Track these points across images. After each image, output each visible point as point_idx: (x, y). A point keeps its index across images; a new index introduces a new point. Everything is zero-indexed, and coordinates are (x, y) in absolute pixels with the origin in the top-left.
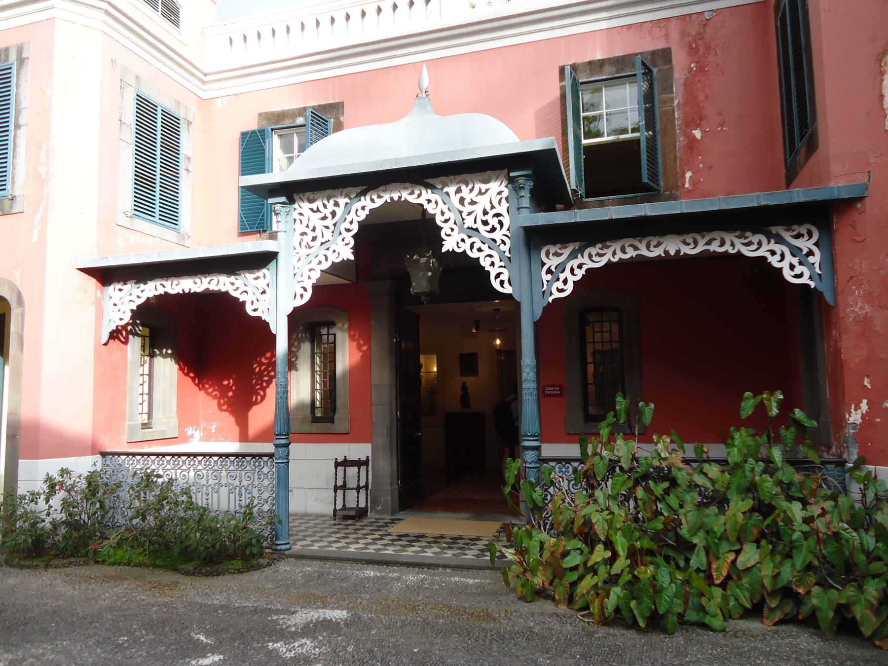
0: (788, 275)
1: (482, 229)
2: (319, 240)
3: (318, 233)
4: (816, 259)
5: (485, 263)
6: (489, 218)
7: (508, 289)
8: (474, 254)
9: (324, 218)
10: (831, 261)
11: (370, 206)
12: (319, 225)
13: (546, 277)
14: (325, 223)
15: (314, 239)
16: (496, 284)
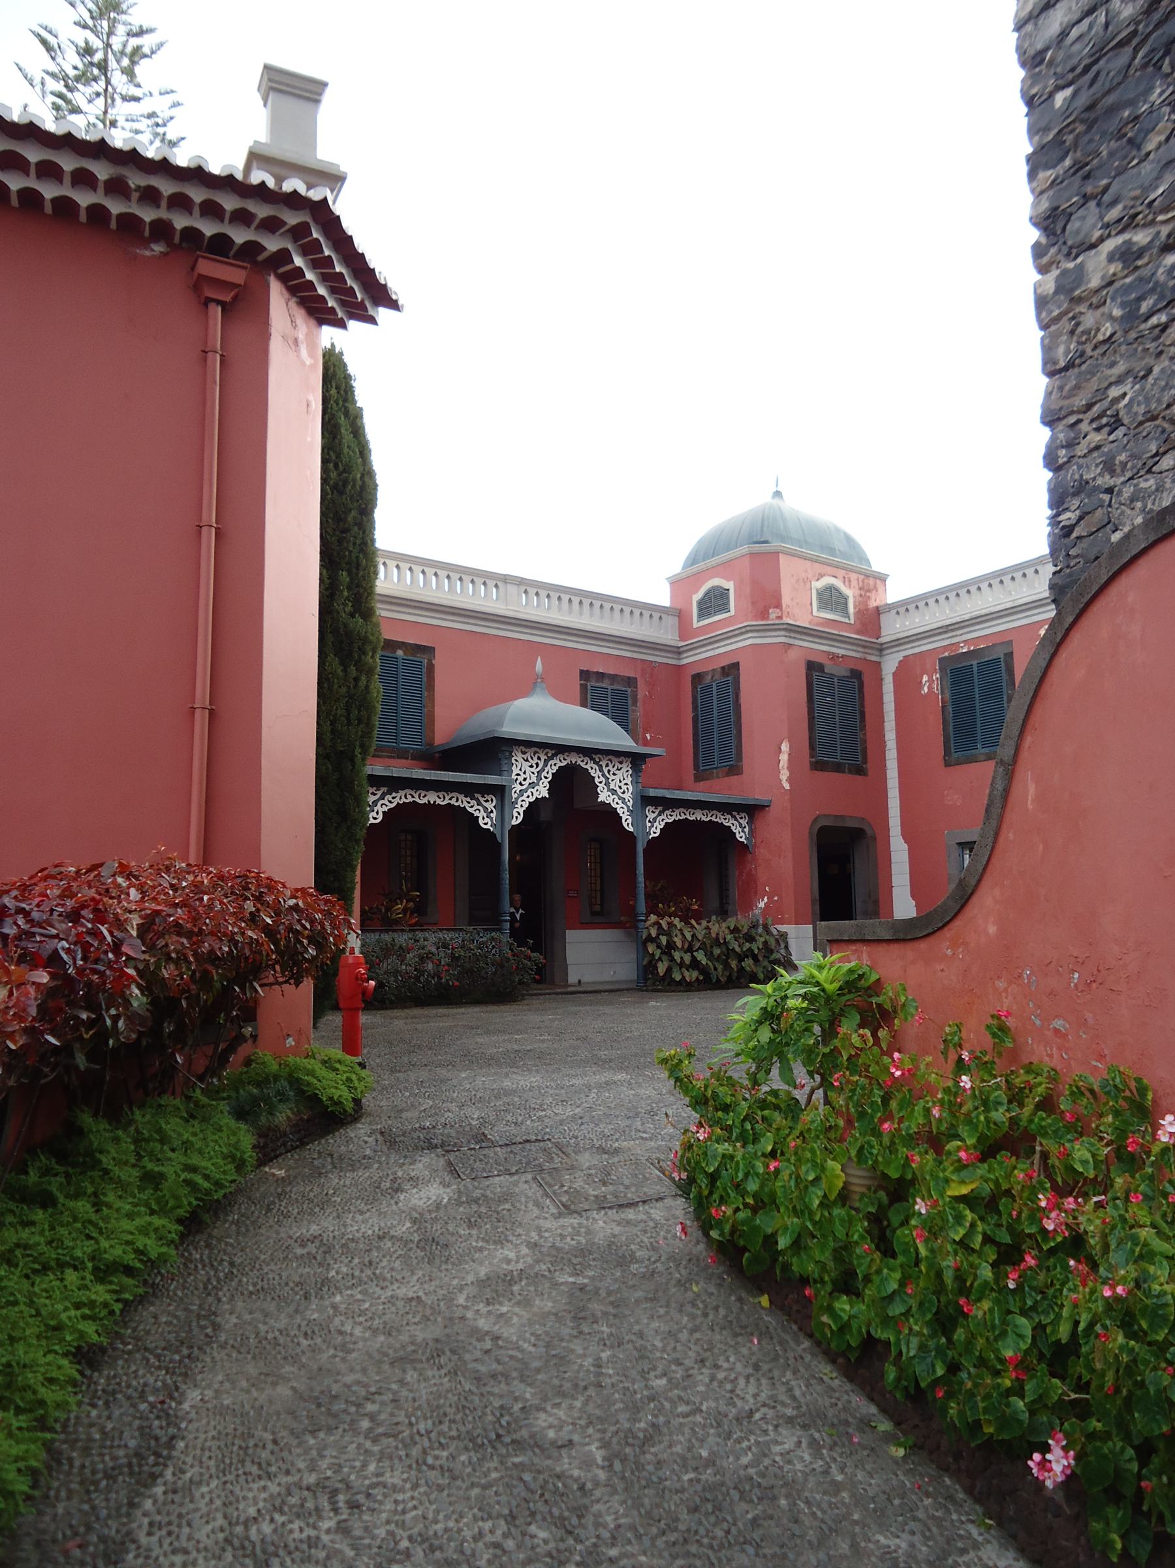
0: (738, 836)
1: (619, 791)
3: (527, 775)
4: (746, 830)
5: (620, 811)
6: (622, 784)
7: (631, 829)
8: (614, 806)
9: (531, 766)
11: (560, 764)
12: (529, 770)
13: (649, 825)
14: (533, 770)
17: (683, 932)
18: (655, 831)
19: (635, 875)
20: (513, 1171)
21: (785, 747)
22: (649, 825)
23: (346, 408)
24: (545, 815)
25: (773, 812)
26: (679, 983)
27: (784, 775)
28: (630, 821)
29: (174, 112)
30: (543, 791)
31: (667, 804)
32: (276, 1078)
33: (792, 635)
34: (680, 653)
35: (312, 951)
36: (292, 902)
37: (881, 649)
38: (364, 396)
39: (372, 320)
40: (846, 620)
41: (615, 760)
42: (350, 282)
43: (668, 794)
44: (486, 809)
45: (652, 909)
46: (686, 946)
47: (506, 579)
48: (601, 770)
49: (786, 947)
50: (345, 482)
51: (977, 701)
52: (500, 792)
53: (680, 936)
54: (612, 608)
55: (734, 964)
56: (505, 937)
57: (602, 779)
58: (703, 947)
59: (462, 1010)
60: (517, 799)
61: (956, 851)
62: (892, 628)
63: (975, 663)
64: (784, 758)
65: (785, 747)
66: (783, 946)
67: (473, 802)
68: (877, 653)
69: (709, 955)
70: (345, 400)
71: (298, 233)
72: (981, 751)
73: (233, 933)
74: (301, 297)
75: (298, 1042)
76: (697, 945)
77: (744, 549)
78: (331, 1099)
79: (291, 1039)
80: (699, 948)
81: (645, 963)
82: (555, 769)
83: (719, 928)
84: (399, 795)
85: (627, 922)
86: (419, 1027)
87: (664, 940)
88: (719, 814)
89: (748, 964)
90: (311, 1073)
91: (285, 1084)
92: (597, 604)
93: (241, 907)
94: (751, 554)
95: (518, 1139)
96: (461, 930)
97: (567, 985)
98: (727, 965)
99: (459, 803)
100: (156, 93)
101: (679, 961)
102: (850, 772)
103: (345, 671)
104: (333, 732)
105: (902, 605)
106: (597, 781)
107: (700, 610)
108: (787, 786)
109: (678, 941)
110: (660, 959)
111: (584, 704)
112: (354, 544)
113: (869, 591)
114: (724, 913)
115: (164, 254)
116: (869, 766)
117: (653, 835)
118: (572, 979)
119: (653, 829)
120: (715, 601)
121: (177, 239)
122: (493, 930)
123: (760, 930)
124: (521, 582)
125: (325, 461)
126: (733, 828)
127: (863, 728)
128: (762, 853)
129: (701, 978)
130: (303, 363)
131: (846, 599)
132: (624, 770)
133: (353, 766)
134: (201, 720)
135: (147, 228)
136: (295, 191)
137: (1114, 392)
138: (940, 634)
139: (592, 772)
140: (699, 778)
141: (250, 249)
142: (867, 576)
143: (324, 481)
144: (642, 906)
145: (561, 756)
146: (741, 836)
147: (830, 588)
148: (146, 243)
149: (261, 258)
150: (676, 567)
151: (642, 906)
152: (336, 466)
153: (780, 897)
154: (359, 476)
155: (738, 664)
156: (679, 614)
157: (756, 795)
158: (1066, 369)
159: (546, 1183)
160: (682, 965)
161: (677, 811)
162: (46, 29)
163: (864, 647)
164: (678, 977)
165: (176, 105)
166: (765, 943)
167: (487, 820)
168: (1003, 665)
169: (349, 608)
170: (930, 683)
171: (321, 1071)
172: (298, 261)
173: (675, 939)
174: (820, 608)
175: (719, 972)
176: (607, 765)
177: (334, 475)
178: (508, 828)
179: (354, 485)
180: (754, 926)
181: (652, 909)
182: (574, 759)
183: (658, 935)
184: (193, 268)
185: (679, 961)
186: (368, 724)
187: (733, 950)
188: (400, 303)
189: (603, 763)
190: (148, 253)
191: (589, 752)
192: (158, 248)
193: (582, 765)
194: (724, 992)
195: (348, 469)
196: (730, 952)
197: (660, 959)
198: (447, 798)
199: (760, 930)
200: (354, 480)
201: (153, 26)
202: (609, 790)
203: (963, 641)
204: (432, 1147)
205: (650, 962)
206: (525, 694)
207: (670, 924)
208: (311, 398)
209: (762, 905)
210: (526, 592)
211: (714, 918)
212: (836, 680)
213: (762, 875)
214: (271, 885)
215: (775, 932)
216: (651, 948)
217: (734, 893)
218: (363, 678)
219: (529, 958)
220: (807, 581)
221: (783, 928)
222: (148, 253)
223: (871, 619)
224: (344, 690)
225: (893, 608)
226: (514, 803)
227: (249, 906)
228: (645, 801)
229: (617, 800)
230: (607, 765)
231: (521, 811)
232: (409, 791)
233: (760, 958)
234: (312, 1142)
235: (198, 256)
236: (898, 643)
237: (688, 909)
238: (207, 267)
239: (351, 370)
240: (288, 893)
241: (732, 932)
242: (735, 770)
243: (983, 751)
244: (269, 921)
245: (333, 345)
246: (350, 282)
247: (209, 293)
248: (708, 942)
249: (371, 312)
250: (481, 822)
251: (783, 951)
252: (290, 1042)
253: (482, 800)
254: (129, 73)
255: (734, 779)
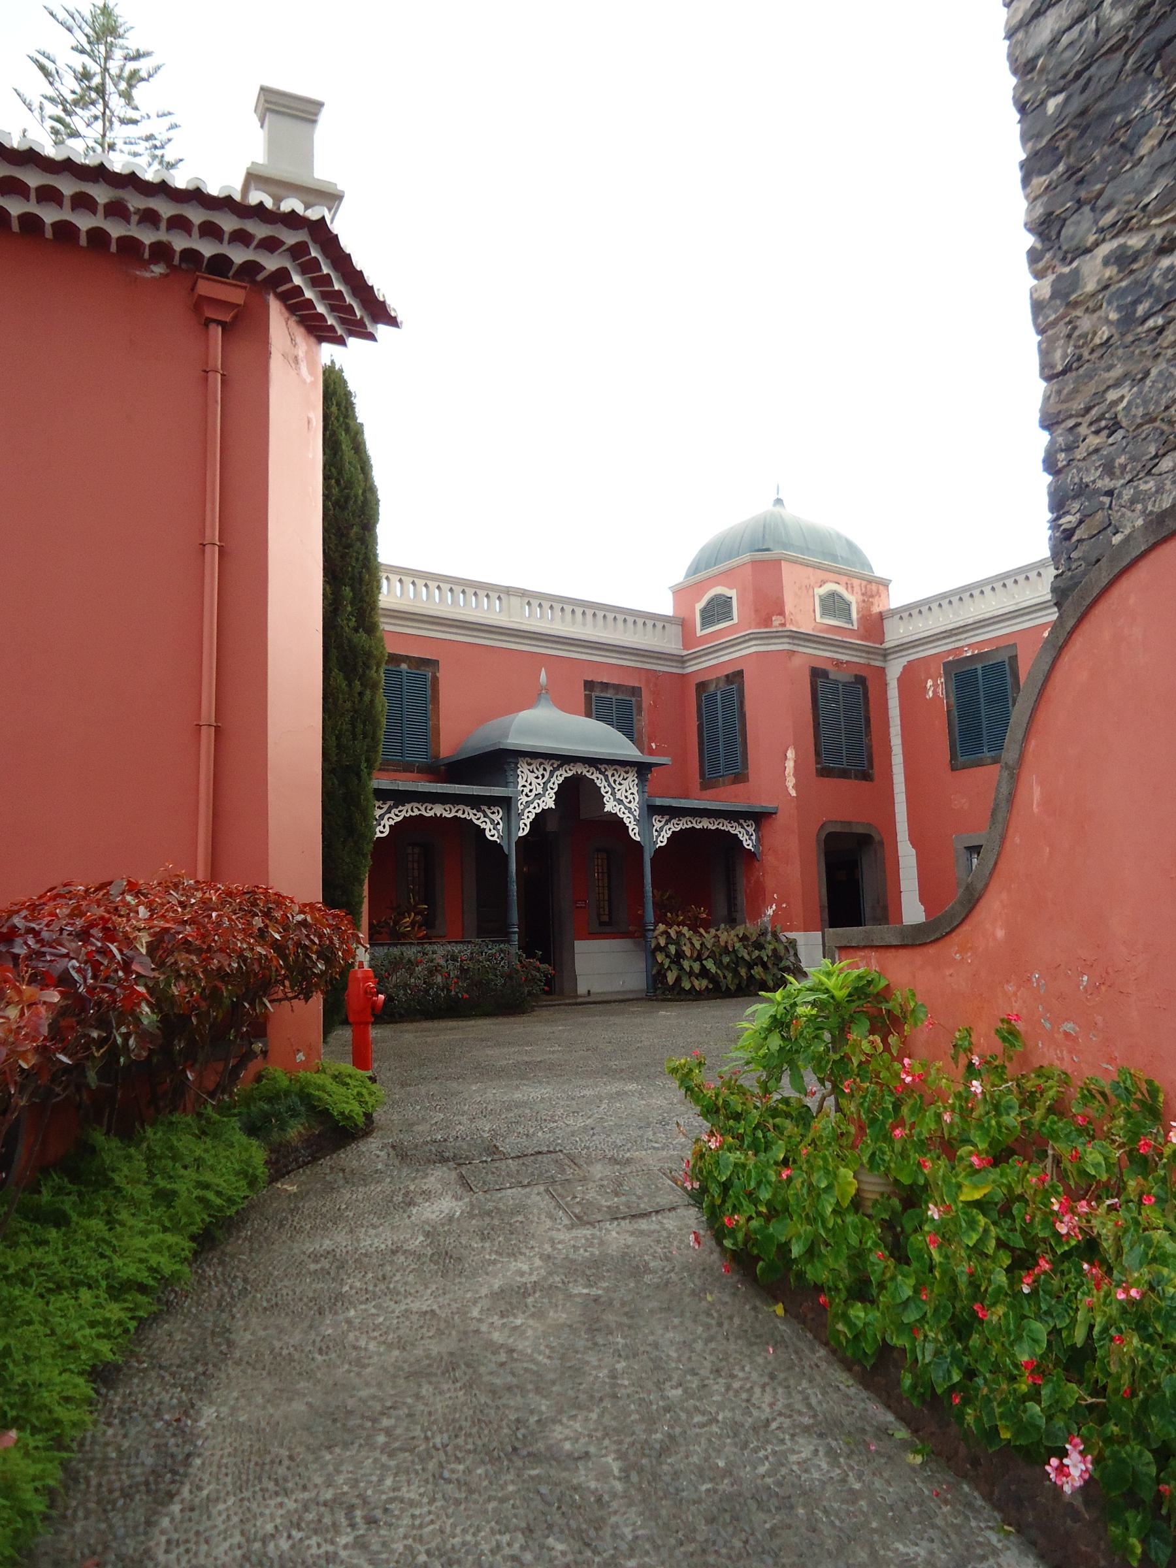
0: (745, 844)
1: (625, 801)
2: (534, 792)
3: (533, 787)
4: (754, 837)
5: (626, 821)
6: (628, 794)
7: (638, 838)
8: (621, 815)
9: (537, 778)
10: (759, 839)
12: (534, 781)
13: (655, 834)
15: (531, 791)
16: (632, 834)
17: (691, 941)
18: (662, 841)
19: (642, 885)
20: (526, 1183)
21: (791, 754)
22: (655, 834)
23: (347, 424)
24: (552, 826)
25: (781, 819)
26: (689, 992)
27: (791, 782)
28: (636, 831)
29: (171, 134)
30: (549, 802)
31: (673, 813)
32: (287, 1093)
33: (796, 642)
34: (684, 662)
35: (321, 966)
36: (300, 917)
37: (885, 654)
38: (364, 412)
39: (371, 337)
40: (850, 626)
41: (621, 770)
42: (349, 300)
43: (674, 803)
44: (492, 821)
45: (659, 919)
46: (695, 955)
47: (509, 591)
48: (607, 780)
49: (796, 954)
50: (347, 498)
51: (982, 705)
52: (506, 803)
53: (689, 945)
54: (615, 618)
55: (743, 972)
56: (514, 949)
57: (608, 789)
58: (712, 955)
59: (472, 1022)
60: (523, 810)
61: (964, 855)
62: (895, 633)
63: (979, 666)
64: (790, 765)
65: (791, 754)
66: (792, 952)
67: (480, 814)
68: (881, 658)
69: (718, 964)
70: (346, 417)
71: (298, 251)
72: (987, 755)
73: (242, 950)
74: (300, 316)
75: (307, 1055)
76: (707, 954)
77: (746, 557)
78: (342, 1113)
79: (301, 1054)
80: (709, 957)
81: (654, 972)
82: (561, 780)
83: (727, 936)
84: (405, 808)
85: (635, 931)
86: (429, 1040)
87: (672, 949)
88: (726, 822)
89: (757, 971)
90: (322, 1088)
91: (296, 1099)
92: (600, 614)
93: (250, 923)
94: (754, 563)
95: (530, 1151)
96: (469, 942)
97: (577, 996)
98: (736, 973)
99: (465, 816)
100: (153, 115)
101: (688, 969)
102: (856, 777)
103: (350, 685)
104: (338, 746)
105: (905, 611)
106: (603, 791)
107: (703, 618)
108: (793, 793)
109: (687, 949)
110: (669, 968)
111: (588, 715)
112: (357, 559)
113: (872, 596)
114: (732, 922)
115: (165, 276)
116: (876, 771)
117: (660, 844)
118: (582, 989)
119: (660, 838)
120: (718, 610)
121: (176, 261)
122: (502, 942)
123: (769, 937)
124: (523, 594)
125: (326, 478)
126: (740, 836)
127: (868, 733)
128: (770, 860)
129: (711, 986)
130: (304, 382)
131: (849, 605)
132: (630, 780)
133: (359, 778)
134: (208, 736)
135: (147, 250)
136: (293, 211)
137: (1112, 395)
138: (944, 638)
139: (598, 783)
140: (706, 784)
141: (252, 268)
142: (870, 582)
143: (326, 497)
144: (650, 916)
145: (566, 767)
146: (748, 844)
147: (833, 595)
148: (145, 265)
149: (260, 277)
150: (678, 575)
151: (650, 916)
152: (338, 482)
153: (788, 904)
154: (360, 492)
155: (742, 672)
156: (684, 624)
157: (763, 803)
158: (1064, 372)
159: (559, 1195)
160: (691, 974)
161: (684, 820)
162: (43, 54)
163: (868, 652)
164: (686, 985)
165: (173, 127)
166: (775, 950)
167: (493, 832)
168: (1007, 668)
169: (353, 623)
170: (935, 688)
171: (332, 1086)
172: (297, 280)
173: (684, 948)
174: (823, 614)
175: (729, 980)
176: (613, 775)
177: (335, 491)
178: (514, 840)
179: (356, 501)
180: (763, 934)
181: (659, 919)
182: (580, 769)
183: (667, 944)
184: (193, 289)
185: (688, 969)
186: (373, 739)
187: (742, 958)
188: (399, 320)
189: (609, 773)
190: (147, 275)
191: (594, 762)
192: (158, 269)
193: (588, 775)
194: (734, 1001)
195: (349, 485)
196: (739, 960)
197: (669, 968)
198: (454, 810)
199: (769, 937)
200: (356, 496)
201: (150, 50)
202: (615, 800)
203: (968, 645)
204: (444, 1160)
205: (659, 972)
206: (529, 706)
207: (679, 933)
208: (312, 415)
209: (770, 912)
210: (529, 603)
211: (723, 926)
212: (840, 686)
213: (770, 883)
214: (280, 900)
215: (784, 939)
216: (660, 957)
217: (742, 900)
218: (368, 692)
219: (538, 969)
220: (809, 588)
221: (792, 935)
222: (147, 275)
223: (874, 625)
224: (348, 705)
225: (897, 613)
226: (520, 815)
227: (258, 922)
228: (652, 810)
229: (623, 810)
230: (613, 775)
231: (528, 822)
232: (415, 805)
233: (770, 966)
234: (324, 1157)
235: (198, 277)
236: (902, 647)
237: (697, 918)
238: (207, 288)
239: (352, 387)
240: (297, 909)
241: (741, 940)
242: (741, 777)
243: (988, 754)
244: (277, 936)
245: (332, 362)
246: (349, 300)
247: (209, 314)
248: (717, 950)
249: (370, 329)
250: (488, 834)
251: (792, 959)
252: (301, 1057)
253: (488, 812)
254: (127, 96)
255: (739, 787)
